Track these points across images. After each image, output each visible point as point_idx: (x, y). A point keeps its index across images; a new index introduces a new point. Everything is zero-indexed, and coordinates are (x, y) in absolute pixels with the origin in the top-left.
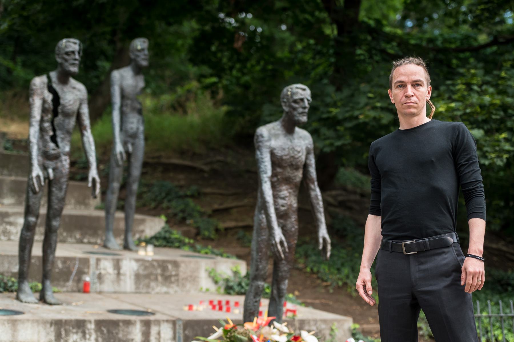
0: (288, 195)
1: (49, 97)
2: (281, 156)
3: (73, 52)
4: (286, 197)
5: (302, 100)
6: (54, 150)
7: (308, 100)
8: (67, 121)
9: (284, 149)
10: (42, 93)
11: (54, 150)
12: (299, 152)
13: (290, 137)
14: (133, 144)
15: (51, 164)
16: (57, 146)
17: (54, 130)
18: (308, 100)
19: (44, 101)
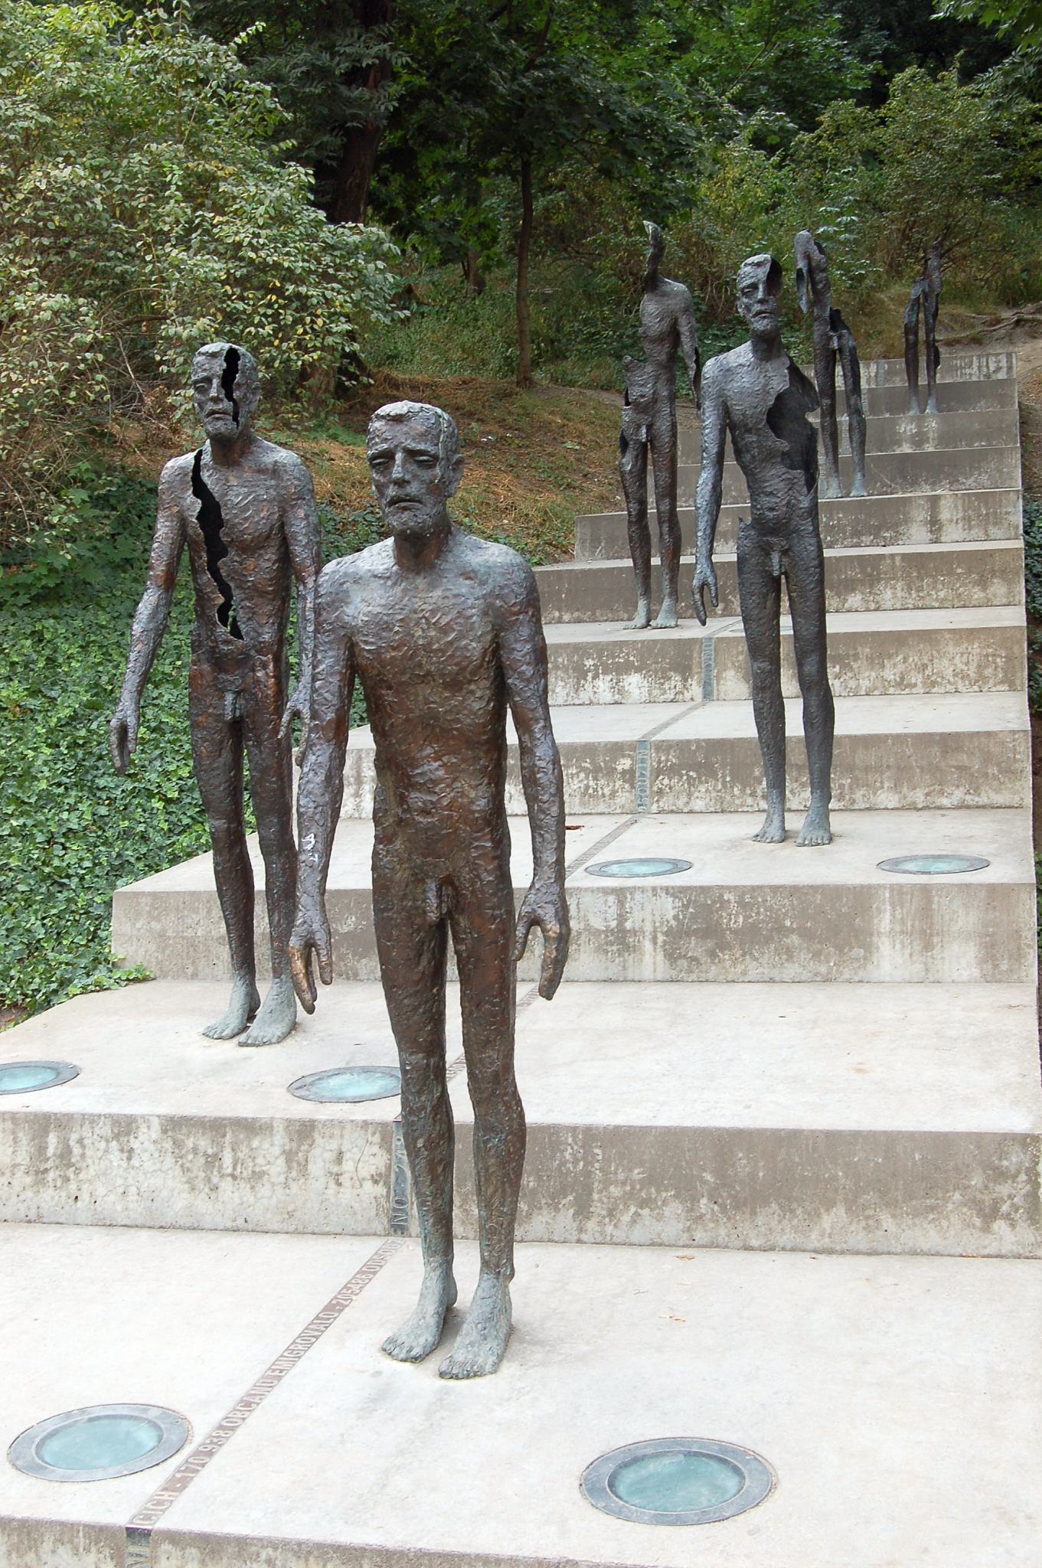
0: (441, 773)
1: (193, 505)
2: (377, 652)
3: (208, 380)
4: (442, 780)
5: (388, 456)
6: (227, 642)
7: (411, 454)
8: (251, 563)
9: (388, 627)
10: (177, 500)
11: (227, 642)
12: (445, 630)
13: (421, 582)
14: (785, 553)
15: (233, 678)
16: (236, 632)
17: (225, 590)
19: (183, 522)
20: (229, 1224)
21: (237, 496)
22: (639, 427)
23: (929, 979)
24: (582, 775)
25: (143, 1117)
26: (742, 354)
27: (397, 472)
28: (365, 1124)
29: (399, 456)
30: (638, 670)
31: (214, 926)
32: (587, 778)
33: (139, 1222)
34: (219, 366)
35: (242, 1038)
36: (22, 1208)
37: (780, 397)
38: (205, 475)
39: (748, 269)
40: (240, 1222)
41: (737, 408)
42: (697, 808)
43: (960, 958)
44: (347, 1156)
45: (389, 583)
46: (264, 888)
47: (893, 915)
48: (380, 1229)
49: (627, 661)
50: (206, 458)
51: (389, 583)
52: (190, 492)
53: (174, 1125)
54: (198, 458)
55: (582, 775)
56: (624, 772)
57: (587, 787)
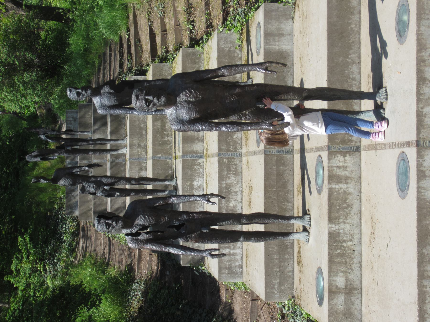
18: (147, 94)
20: (359, 201)
21: (141, 221)
22: (104, 189)
23: (291, 34)
24: (229, 175)
25: (328, 229)
26: (96, 101)
27: (150, 98)
28: (329, 159)
29: (147, 97)
30: (192, 181)
31: (274, 243)
32: (230, 174)
33: (360, 229)
34: (102, 221)
35: (307, 226)
36: (357, 269)
37: (111, 88)
38: (134, 231)
39: (71, 95)
40: (358, 198)
41: (113, 102)
42: (241, 137)
43: (286, 26)
44: (338, 165)
45: (178, 108)
46: (263, 226)
47: (273, 45)
48: (359, 154)
49: (189, 186)
50: (128, 231)
51: (178, 108)
52: (139, 237)
53: (331, 220)
54: (127, 235)
55: (229, 175)
56: (228, 161)
57: (233, 174)
